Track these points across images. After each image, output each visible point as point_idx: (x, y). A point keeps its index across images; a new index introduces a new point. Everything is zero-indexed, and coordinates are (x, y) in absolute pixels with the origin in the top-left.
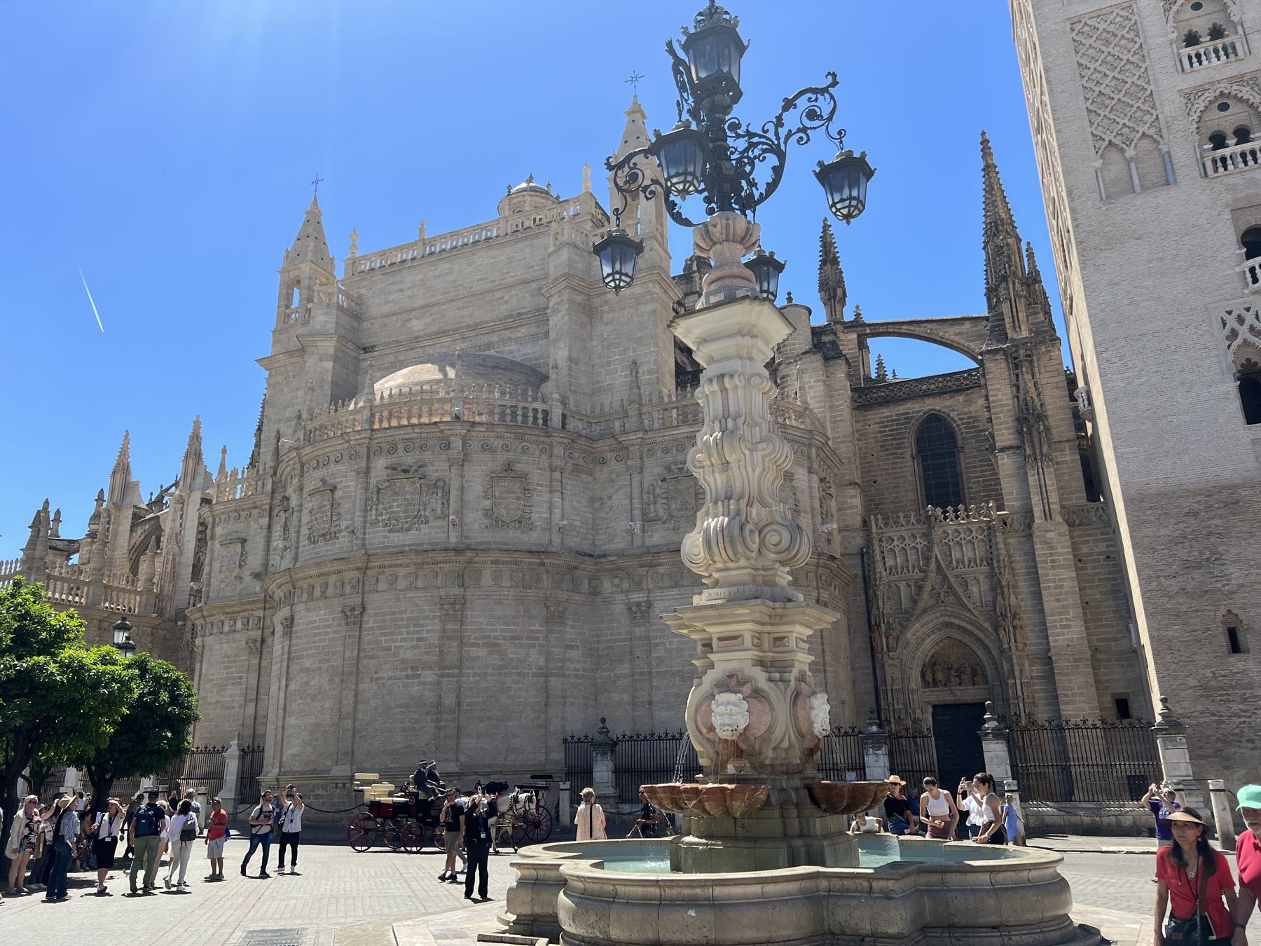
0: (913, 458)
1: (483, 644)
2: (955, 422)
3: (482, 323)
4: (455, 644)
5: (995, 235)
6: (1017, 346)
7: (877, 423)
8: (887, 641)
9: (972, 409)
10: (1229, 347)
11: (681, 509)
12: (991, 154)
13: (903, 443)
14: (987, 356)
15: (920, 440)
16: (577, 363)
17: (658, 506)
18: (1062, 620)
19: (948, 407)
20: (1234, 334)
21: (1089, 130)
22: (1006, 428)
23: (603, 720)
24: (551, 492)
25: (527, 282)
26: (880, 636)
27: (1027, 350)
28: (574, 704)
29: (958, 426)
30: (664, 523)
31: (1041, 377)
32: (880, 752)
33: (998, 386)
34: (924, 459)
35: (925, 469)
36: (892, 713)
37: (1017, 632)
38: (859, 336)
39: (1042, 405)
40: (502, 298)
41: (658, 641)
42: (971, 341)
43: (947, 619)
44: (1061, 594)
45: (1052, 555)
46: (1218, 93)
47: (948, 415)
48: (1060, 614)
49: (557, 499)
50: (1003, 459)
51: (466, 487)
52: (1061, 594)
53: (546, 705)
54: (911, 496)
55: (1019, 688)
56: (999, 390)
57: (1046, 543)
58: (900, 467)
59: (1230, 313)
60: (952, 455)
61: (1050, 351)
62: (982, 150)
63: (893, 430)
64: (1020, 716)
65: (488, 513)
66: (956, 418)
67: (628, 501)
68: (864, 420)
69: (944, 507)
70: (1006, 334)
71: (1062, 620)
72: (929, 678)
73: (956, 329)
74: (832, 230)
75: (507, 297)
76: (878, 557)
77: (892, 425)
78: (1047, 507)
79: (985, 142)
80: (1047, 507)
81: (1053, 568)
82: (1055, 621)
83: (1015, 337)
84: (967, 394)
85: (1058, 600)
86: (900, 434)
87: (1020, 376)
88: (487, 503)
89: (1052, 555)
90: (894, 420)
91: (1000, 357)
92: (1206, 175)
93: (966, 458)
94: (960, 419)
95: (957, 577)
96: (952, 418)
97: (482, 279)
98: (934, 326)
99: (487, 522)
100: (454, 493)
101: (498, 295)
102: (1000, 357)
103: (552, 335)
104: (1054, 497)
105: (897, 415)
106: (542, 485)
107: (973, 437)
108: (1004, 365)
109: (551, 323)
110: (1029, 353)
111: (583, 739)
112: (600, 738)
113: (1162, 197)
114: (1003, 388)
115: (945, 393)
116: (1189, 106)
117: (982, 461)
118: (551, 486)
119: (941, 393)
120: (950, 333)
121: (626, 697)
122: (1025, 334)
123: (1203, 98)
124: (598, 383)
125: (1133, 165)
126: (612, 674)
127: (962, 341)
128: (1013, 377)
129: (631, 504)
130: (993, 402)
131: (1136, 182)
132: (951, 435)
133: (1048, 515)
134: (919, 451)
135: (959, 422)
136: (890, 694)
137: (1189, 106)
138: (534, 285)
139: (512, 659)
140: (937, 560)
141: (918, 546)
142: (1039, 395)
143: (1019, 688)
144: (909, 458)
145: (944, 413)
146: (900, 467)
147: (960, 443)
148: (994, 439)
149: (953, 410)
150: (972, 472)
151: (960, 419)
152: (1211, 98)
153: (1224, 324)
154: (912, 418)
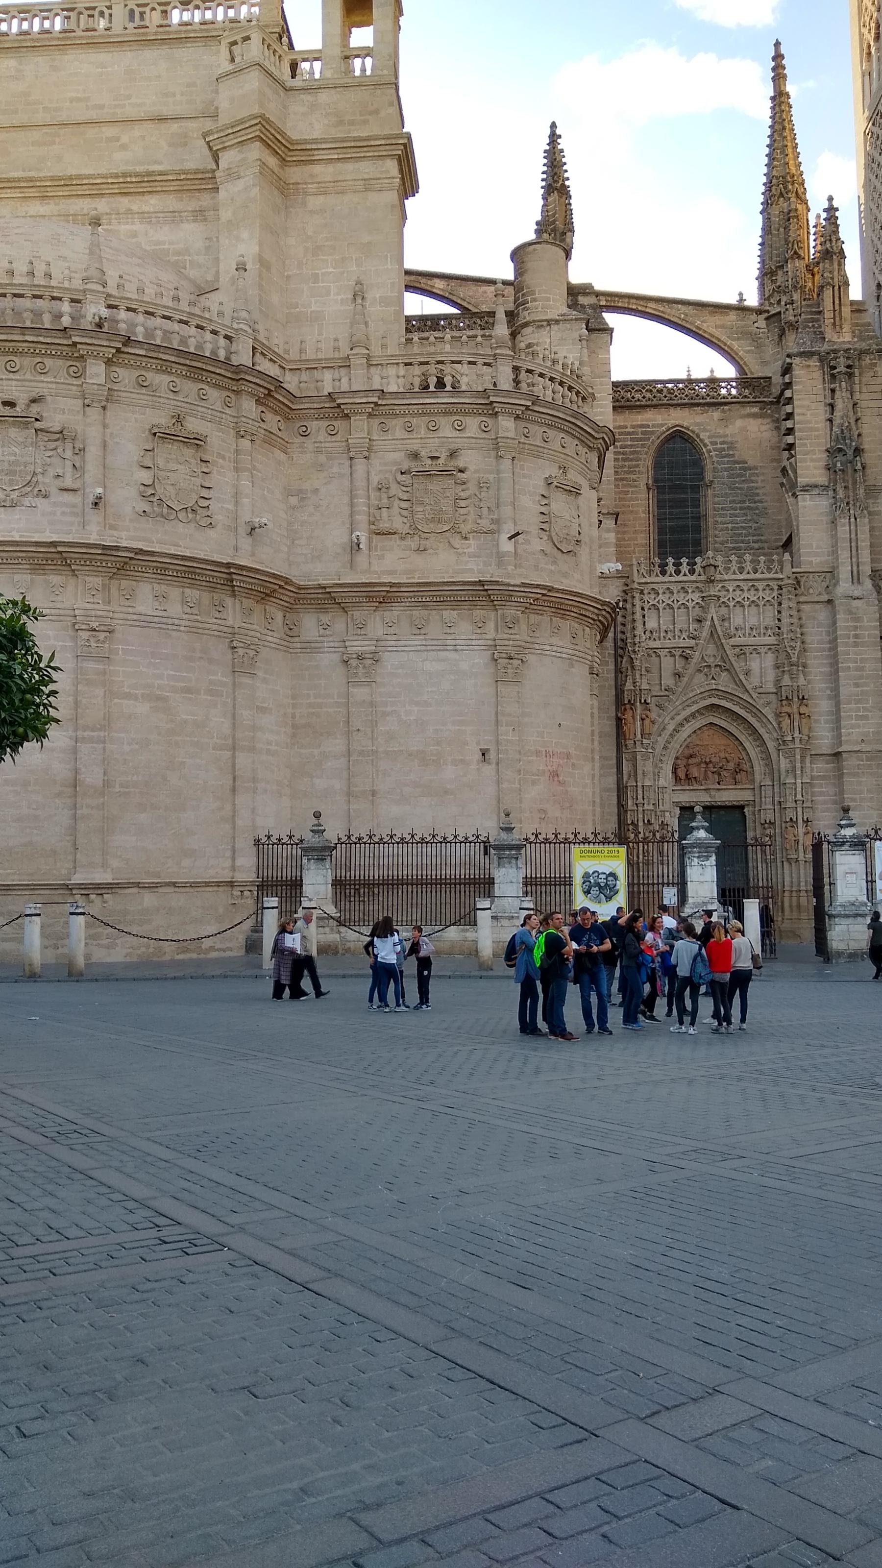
0: (649, 489)
1: (143, 695)
2: (705, 445)
3: (79, 177)
4: (100, 692)
5: (781, 195)
6: (835, 351)
8: (642, 725)
9: (729, 430)
11: (432, 520)
12: (784, 77)
13: (637, 466)
14: (797, 361)
15: (657, 466)
16: (268, 269)
17: (395, 510)
18: (858, 710)
19: (697, 424)
22: (812, 460)
23: (317, 815)
24: (237, 470)
25: (162, 119)
26: (633, 717)
27: (848, 358)
28: (266, 791)
29: (709, 451)
30: (402, 539)
31: (863, 396)
32: (707, 863)
33: (806, 403)
34: (660, 490)
35: (660, 504)
36: (641, 816)
37: (804, 721)
39: (859, 435)
41: (389, 709)
42: (734, 339)
43: (715, 701)
44: (861, 677)
45: (856, 628)
47: (698, 436)
48: (858, 702)
49: (245, 483)
50: (804, 500)
51: (110, 442)
52: (861, 677)
53: (234, 790)
54: (642, 539)
55: (799, 789)
56: (808, 408)
57: (851, 613)
58: (631, 499)
60: (696, 489)
61: (875, 365)
62: (773, 69)
63: (626, 446)
64: (796, 822)
65: (148, 492)
66: (707, 441)
67: (346, 500)
69: (677, 558)
71: (858, 710)
72: (681, 774)
73: (718, 319)
74: (563, 144)
75: (125, 139)
76: (638, 616)
77: (625, 440)
78: (855, 568)
79: (778, 57)
80: (855, 568)
81: (856, 645)
82: (850, 710)
83: (835, 338)
84: (723, 411)
85: (857, 685)
86: (632, 453)
87: (838, 394)
88: (145, 477)
89: (856, 628)
90: (629, 433)
91: (814, 362)
93: (715, 496)
94: (713, 443)
96: (702, 440)
97: (78, 100)
98: (690, 310)
99: (143, 506)
100: (93, 452)
101: (109, 131)
102: (814, 362)
103: (226, 214)
104: (865, 555)
105: (633, 427)
106: (223, 458)
107: (726, 470)
108: (818, 374)
109: (222, 194)
110: (850, 362)
111: (285, 840)
112: (311, 840)
114: (813, 406)
115: (698, 405)
117: (734, 502)
118: (236, 461)
119: (692, 404)
120: (709, 324)
121: (338, 785)
122: (847, 337)
124: (296, 306)
126: (316, 752)
127: (723, 338)
128: (828, 393)
129: (352, 505)
130: (800, 422)
132: (698, 464)
133: (856, 578)
134: (656, 480)
135: (710, 447)
136: (640, 792)
138: (174, 127)
139: (186, 721)
140: (713, 625)
141: (690, 605)
142: (857, 420)
143: (799, 789)
144: (643, 488)
145: (693, 432)
146: (631, 499)
147: (709, 476)
148: (795, 472)
149: (705, 430)
150: (721, 516)
151: (713, 443)
154: (652, 433)
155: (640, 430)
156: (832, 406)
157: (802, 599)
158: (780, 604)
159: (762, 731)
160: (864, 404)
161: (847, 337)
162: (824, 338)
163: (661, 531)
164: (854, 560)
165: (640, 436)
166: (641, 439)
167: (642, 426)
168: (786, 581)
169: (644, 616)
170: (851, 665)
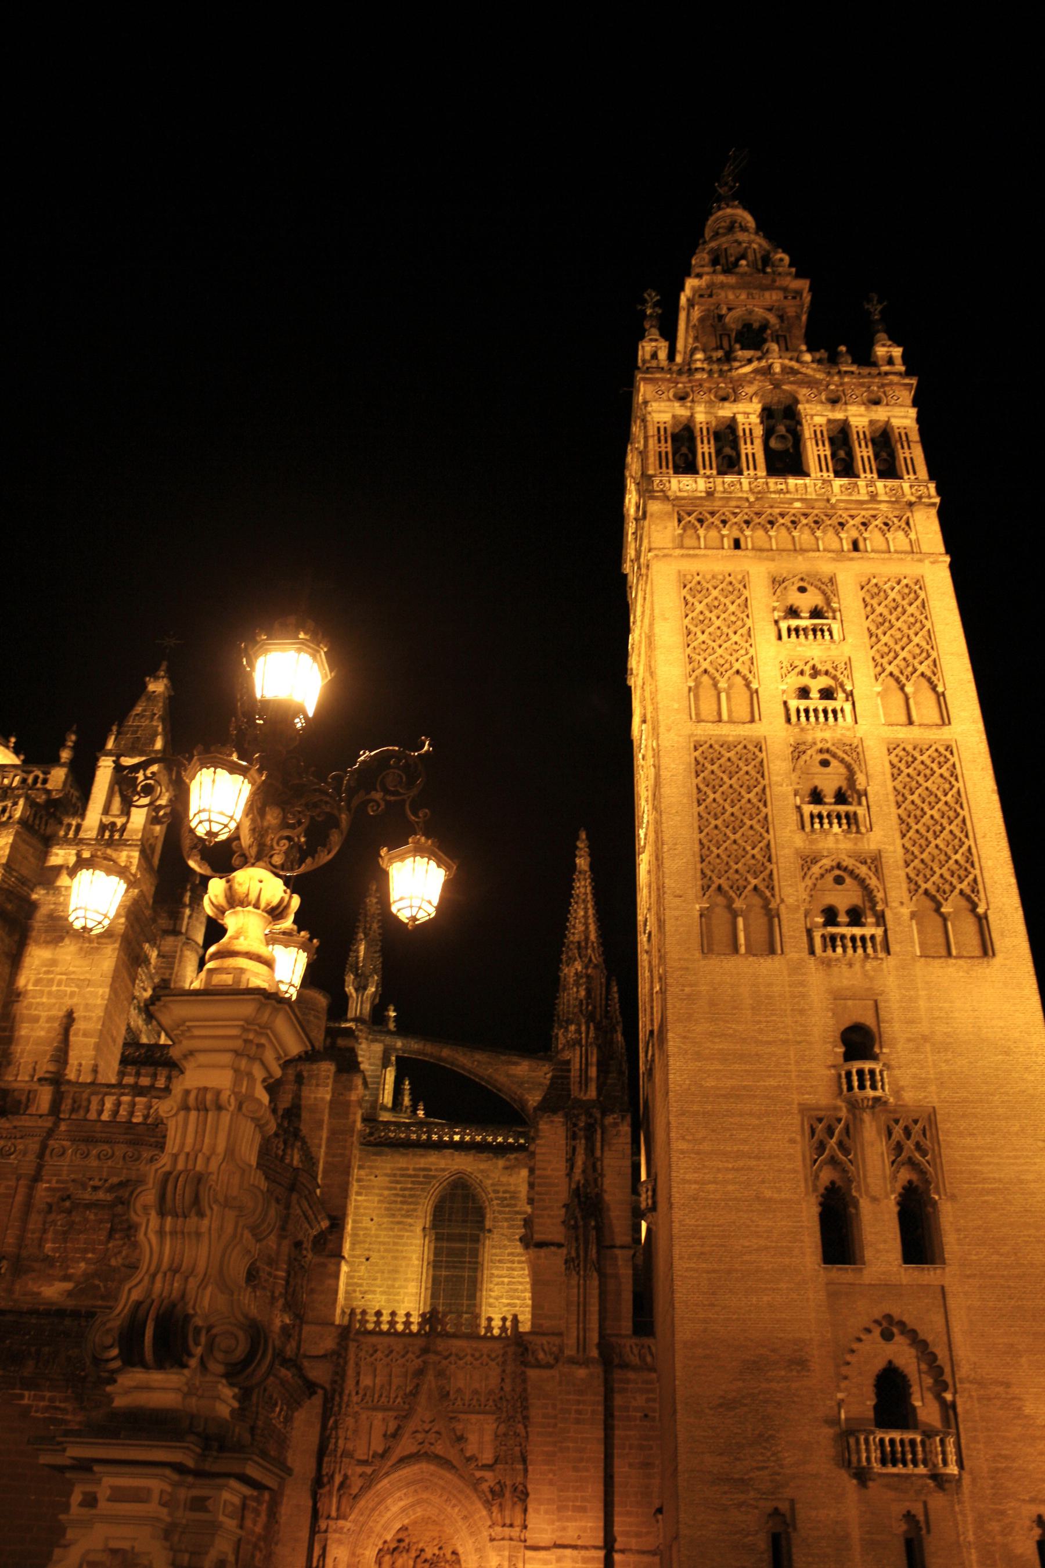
10: (816, 1161)
20: (821, 1147)
21: (699, 866)
46: (834, 864)
59: (820, 1120)
68: (371, 1167)
70: (569, 1090)
76: (351, 1372)
81: (578, 1421)
85: (576, 1469)
92: (812, 952)
113: (768, 966)
116: (806, 869)
123: (820, 864)
125: (740, 921)
130: (539, 1177)
131: (742, 939)
137: (806, 869)
152: (828, 867)
153: (813, 1132)
160: (606, 1162)
161: (592, 1093)
162: (570, 1095)
164: (581, 1326)
169: (358, 1374)
170: (571, 1445)
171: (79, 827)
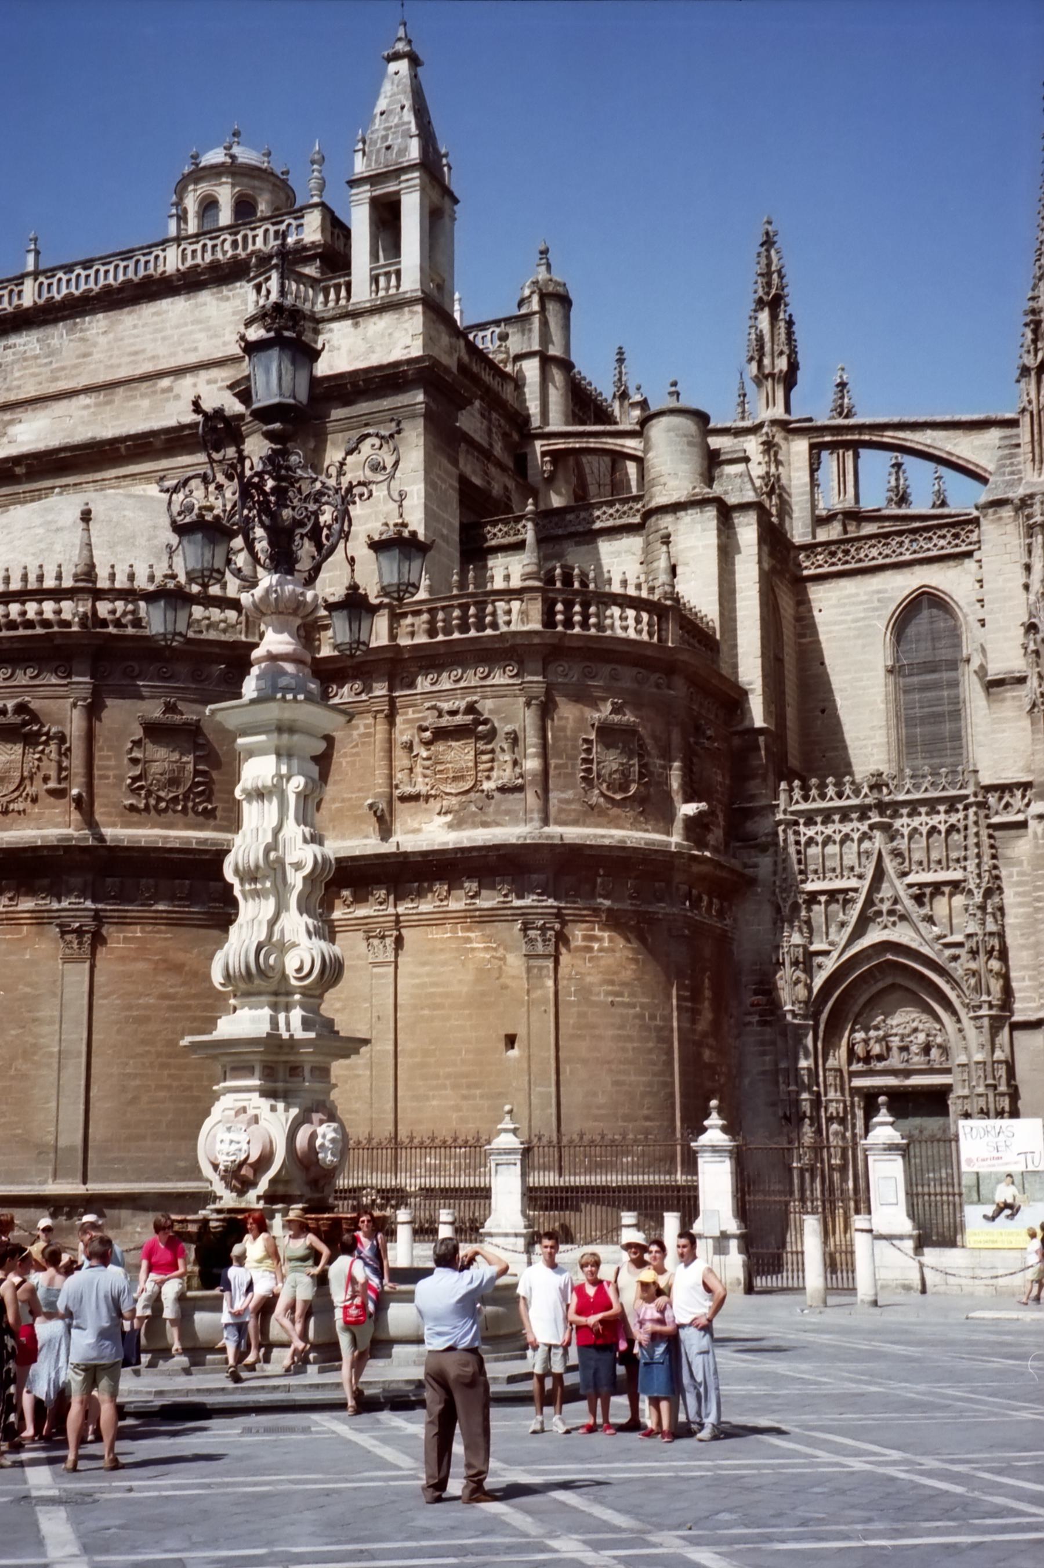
7: (835, 606)
38: (812, 446)
40: (170, 389)
60: (953, 665)
90: (862, 603)
95: (910, 886)
105: (866, 593)
108: (1011, 528)
128: (1023, 552)
132: (954, 635)
134: (897, 659)
144: (881, 672)
155: (876, 597)
156: (1028, 568)
157: (996, 820)
158: (966, 828)
159: (952, 995)
163: (910, 722)
165: (876, 604)
166: (875, 609)
167: (879, 592)
168: (972, 799)
171: (348, 286)
